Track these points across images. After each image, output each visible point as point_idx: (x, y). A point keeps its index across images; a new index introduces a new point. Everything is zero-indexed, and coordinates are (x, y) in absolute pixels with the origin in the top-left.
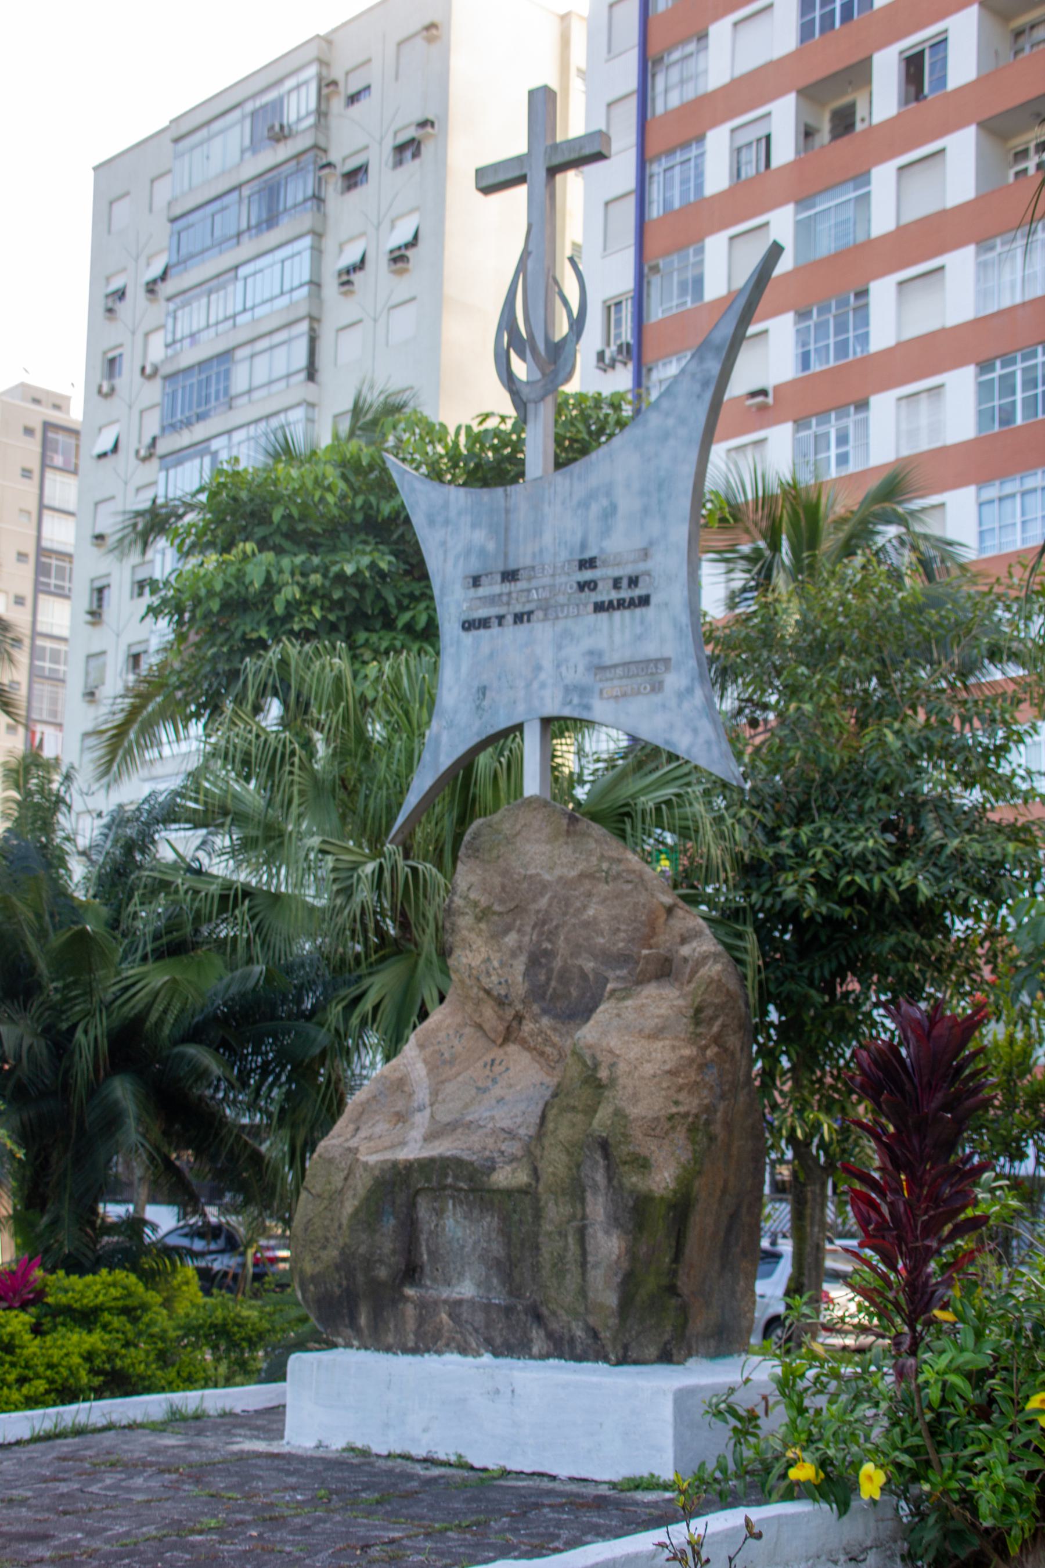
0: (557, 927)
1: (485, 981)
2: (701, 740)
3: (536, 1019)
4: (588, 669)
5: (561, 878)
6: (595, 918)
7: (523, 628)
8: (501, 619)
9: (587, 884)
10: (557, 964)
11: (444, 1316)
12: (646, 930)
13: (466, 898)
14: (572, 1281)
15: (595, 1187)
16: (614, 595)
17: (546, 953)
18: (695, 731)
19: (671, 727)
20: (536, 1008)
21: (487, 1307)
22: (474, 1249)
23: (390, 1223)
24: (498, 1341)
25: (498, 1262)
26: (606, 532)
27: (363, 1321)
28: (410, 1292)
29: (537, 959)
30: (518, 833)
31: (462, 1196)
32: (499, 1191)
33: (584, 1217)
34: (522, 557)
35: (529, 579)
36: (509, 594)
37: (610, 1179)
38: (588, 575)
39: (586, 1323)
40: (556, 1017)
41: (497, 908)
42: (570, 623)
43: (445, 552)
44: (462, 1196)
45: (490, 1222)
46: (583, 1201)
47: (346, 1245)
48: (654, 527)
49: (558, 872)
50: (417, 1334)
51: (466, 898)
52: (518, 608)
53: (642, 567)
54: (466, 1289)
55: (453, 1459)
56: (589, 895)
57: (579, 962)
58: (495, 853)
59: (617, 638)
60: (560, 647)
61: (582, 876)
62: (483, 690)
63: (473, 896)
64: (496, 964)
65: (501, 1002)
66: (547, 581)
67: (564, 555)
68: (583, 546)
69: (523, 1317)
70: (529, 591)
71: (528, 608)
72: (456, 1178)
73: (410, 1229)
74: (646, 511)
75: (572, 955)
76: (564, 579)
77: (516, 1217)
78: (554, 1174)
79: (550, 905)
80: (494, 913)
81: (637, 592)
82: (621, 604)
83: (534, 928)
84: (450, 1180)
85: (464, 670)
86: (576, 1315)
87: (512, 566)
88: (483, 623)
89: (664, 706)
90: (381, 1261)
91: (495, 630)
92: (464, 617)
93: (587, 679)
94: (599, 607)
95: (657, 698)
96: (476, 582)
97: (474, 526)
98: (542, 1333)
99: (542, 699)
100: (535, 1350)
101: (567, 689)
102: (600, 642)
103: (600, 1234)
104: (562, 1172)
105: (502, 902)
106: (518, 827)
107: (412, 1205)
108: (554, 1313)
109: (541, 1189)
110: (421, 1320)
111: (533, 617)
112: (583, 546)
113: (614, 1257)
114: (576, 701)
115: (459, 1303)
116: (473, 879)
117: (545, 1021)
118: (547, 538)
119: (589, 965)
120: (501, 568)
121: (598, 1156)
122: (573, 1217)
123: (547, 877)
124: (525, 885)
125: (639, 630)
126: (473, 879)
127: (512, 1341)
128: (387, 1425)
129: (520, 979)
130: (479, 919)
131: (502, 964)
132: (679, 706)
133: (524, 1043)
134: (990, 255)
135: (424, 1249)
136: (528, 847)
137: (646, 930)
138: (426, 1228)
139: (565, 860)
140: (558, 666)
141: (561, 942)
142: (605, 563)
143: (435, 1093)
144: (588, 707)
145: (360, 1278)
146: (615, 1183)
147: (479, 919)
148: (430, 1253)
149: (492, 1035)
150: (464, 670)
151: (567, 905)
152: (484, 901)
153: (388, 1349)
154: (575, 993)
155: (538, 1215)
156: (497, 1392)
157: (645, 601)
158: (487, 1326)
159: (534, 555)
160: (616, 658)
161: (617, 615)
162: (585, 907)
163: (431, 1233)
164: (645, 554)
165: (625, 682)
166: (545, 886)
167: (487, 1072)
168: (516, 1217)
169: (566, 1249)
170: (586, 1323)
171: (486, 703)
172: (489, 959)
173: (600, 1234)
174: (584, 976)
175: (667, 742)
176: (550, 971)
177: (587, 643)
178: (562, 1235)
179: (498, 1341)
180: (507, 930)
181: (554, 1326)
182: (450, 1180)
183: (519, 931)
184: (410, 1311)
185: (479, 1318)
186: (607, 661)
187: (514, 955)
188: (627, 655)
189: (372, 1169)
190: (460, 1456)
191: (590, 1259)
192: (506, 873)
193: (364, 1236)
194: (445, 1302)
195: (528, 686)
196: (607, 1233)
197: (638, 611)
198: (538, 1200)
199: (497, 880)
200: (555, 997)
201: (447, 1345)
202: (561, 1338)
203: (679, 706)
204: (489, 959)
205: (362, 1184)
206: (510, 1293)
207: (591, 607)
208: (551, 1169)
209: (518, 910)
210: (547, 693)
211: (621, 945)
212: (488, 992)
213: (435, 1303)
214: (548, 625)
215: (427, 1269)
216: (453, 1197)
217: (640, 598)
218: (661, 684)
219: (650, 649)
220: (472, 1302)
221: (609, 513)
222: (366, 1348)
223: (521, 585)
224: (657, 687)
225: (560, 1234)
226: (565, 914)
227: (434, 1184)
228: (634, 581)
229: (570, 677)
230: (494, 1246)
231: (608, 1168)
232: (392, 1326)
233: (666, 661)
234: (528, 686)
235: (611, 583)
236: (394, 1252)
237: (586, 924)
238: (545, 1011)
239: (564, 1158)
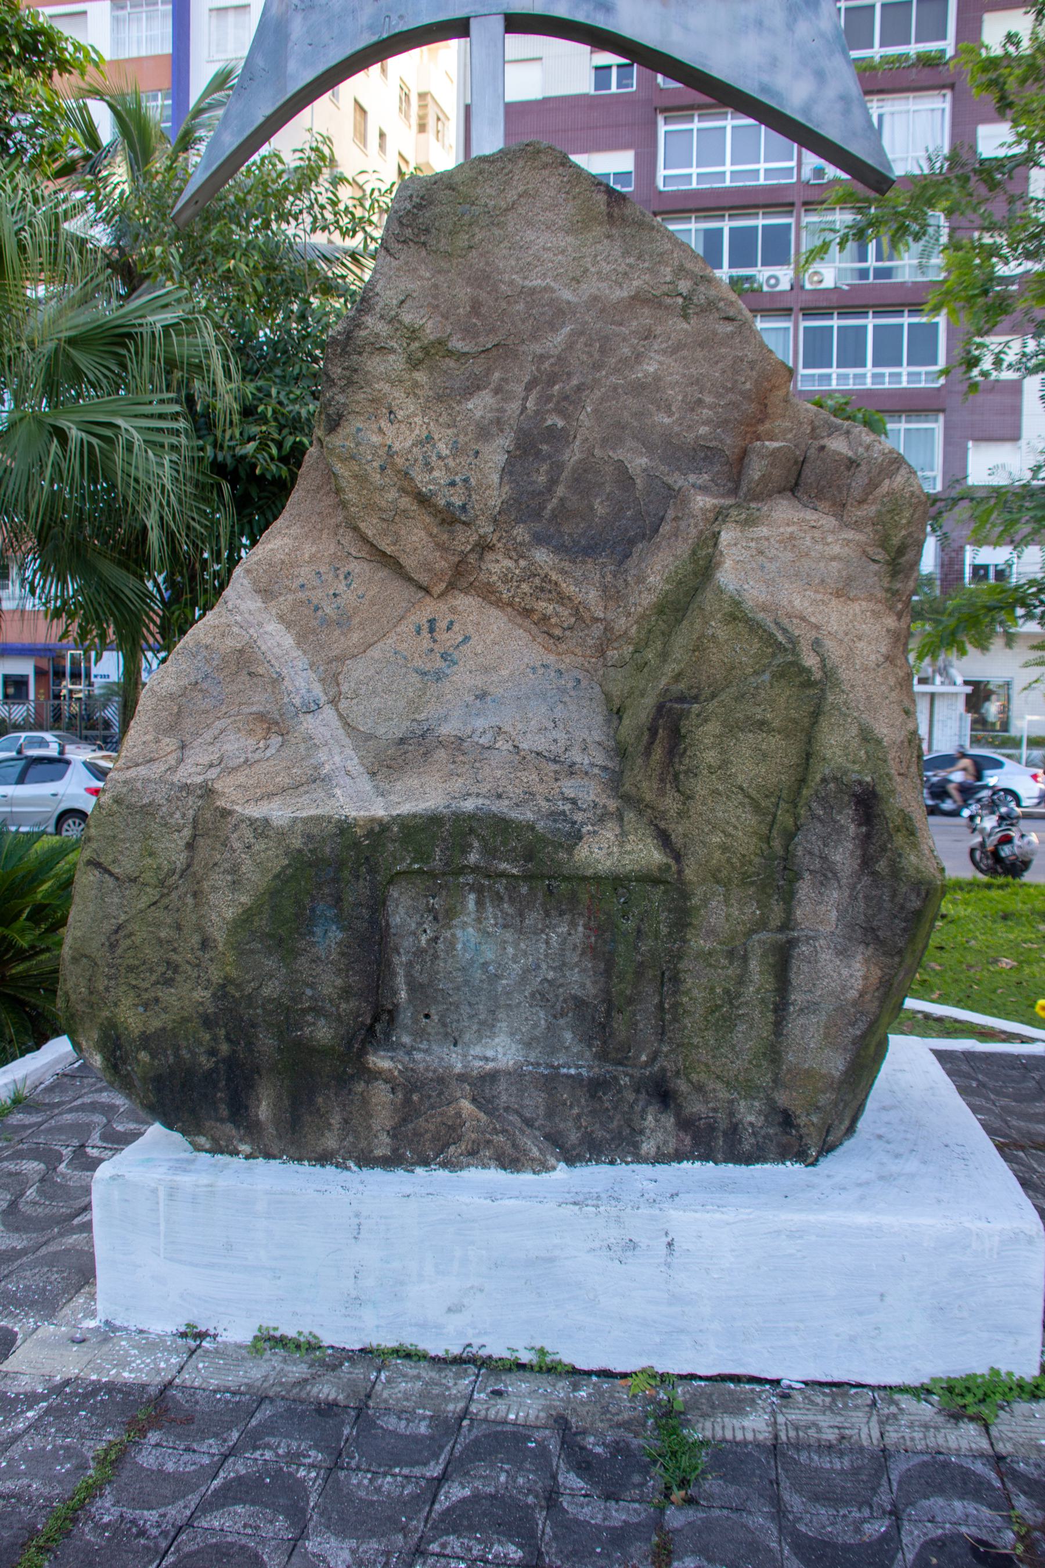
0: (579, 388)
1: (422, 480)
2: (831, 92)
3: (518, 551)
5: (596, 298)
6: (657, 378)
9: (645, 316)
10: (573, 455)
11: (466, 1105)
12: (751, 408)
13: (393, 320)
14: (749, 1036)
15: (827, 874)
17: (553, 435)
18: (820, 76)
19: (774, 63)
20: (521, 533)
21: (550, 1082)
22: (523, 980)
23: (330, 939)
24: (574, 1137)
25: (580, 1003)
27: (264, 1111)
28: (381, 1061)
29: (531, 446)
30: (512, 207)
31: (500, 886)
32: (597, 879)
33: (786, 926)
37: (867, 862)
39: (771, 1102)
40: (560, 549)
41: (457, 344)
44: (500, 886)
45: (566, 934)
46: (788, 897)
47: (228, 980)
49: (590, 287)
50: (394, 1133)
51: (393, 320)
54: (501, 1051)
55: (525, 1357)
56: (648, 335)
57: (619, 454)
61: (638, 299)
63: (407, 318)
64: (443, 449)
65: (449, 519)
69: (631, 1096)
72: (490, 852)
73: (373, 945)
75: (604, 441)
77: (630, 925)
78: (724, 848)
79: (570, 346)
80: (450, 353)
83: (529, 388)
84: (473, 858)
86: (749, 1089)
89: (759, 24)
90: (317, 1011)
98: (669, 1121)
100: (648, 1147)
103: (826, 956)
104: (746, 843)
105: (469, 332)
106: (512, 195)
107: (378, 904)
108: (700, 1088)
109: (689, 874)
110: (407, 1112)
113: (853, 994)
115: (492, 1077)
116: (408, 284)
117: (542, 556)
119: (638, 462)
121: (847, 819)
122: (762, 924)
123: (567, 295)
124: (520, 307)
126: (408, 284)
127: (599, 1134)
128: (358, 1301)
129: (495, 478)
130: (414, 364)
131: (457, 450)
132: (790, 27)
133: (488, 594)
134: (121, 13)
135: (401, 981)
136: (530, 235)
137: (751, 408)
138: (407, 943)
139: (606, 268)
141: (585, 417)
143: (332, 680)
145: (266, 1042)
146: (882, 866)
147: (414, 364)
148: (414, 987)
149: (423, 578)
151: (602, 351)
152: (432, 330)
153: (323, 1159)
154: (601, 509)
155: (682, 919)
156: (632, 1245)
158: (550, 1114)
162: (639, 357)
163: (420, 952)
166: (560, 312)
167: (426, 644)
168: (630, 925)
169: (741, 981)
170: (771, 1102)
172: (429, 438)
173: (826, 956)
174: (624, 478)
175: (765, 89)
176: (559, 466)
178: (737, 955)
179: (574, 1137)
180: (471, 390)
181: (696, 1107)
182: (473, 858)
183: (497, 391)
184: (381, 1095)
185: (535, 1102)
187: (484, 433)
189: (282, 834)
190: (542, 1352)
191: (797, 997)
192: (482, 279)
193: (270, 963)
194: (462, 1078)
196: (842, 953)
198: (685, 896)
199: (464, 293)
200: (562, 513)
201: (472, 1153)
202: (712, 1128)
203: (790, 27)
204: (429, 438)
205: (260, 866)
206: (603, 1056)
208: (716, 839)
209: (502, 351)
211: (703, 430)
212: (423, 500)
213: (441, 1080)
215: (405, 1017)
216: (479, 890)
220: (516, 1075)
222: (268, 1156)
225: (731, 954)
226: (597, 367)
227: (437, 863)
230: (574, 976)
231: (866, 840)
232: (336, 1120)
236: (346, 993)
237: (639, 388)
238: (539, 540)
239: (749, 818)
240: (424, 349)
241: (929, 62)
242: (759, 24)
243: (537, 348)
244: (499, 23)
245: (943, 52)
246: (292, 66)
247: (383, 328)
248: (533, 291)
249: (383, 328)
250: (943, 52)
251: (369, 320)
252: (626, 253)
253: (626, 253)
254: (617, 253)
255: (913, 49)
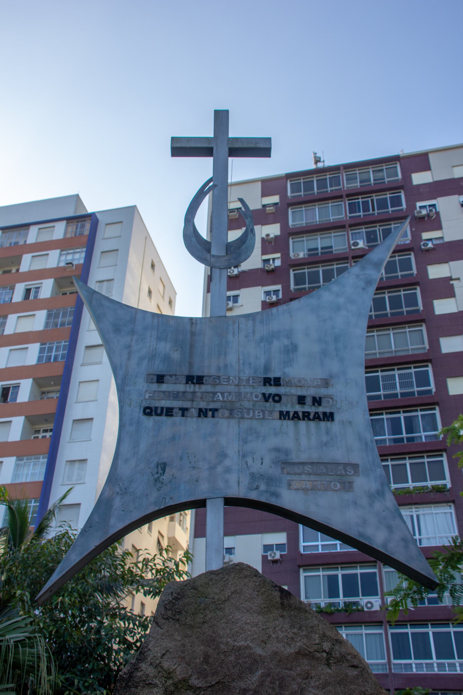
4: (276, 462)
5: (276, 653)
7: (206, 423)
8: (184, 411)
13: (158, 666)
16: (298, 408)
19: (365, 522)
26: (288, 362)
30: (228, 599)
34: (208, 367)
35: (214, 385)
36: (194, 393)
38: (273, 390)
41: (194, 681)
42: (255, 424)
43: (130, 353)
48: (334, 366)
49: (273, 646)
51: (158, 666)
52: (203, 405)
53: (322, 392)
56: (307, 677)
58: (200, 618)
59: (304, 442)
60: (245, 442)
61: (300, 654)
62: (163, 467)
63: (166, 665)
66: (231, 388)
67: (247, 373)
68: (267, 368)
70: (214, 393)
71: (212, 406)
74: (324, 353)
76: (248, 390)
79: (262, 684)
80: (190, 687)
81: (321, 410)
82: (306, 416)
85: (143, 446)
87: (196, 372)
88: (169, 412)
91: (178, 419)
92: (145, 404)
93: (275, 471)
94: (284, 415)
95: (348, 496)
96: (160, 379)
97: (159, 339)
99: (227, 481)
101: (253, 476)
102: (288, 442)
105: (202, 674)
106: (227, 593)
111: (220, 413)
112: (267, 368)
114: (263, 487)
118: (232, 358)
120: (186, 373)
123: (259, 651)
124: (232, 658)
125: (325, 438)
134: (20, 462)
139: (281, 635)
140: (244, 456)
142: (289, 384)
144: (276, 495)
150: (143, 446)
151: (281, 686)
152: (180, 672)
157: (329, 417)
159: (219, 369)
160: (303, 457)
161: (302, 424)
164: (326, 383)
165: (313, 477)
166: (256, 662)
171: (166, 477)
175: (361, 535)
177: (273, 442)
186: (294, 458)
188: (314, 456)
195: (212, 468)
197: (323, 424)
199: (200, 649)
207: (277, 415)
210: (233, 478)
214: (233, 422)
217: (325, 414)
218: (351, 483)
219: (337, 454)
221: (291, 350)
223: (204, 388)
224: (348, 486)
228: (317, 401)
229: (256, 467)
233: (355, 466)
234: (212, 468)
235: (295, 399)
240: (175, 684)
241: (439, 490)
242: (355, 503)
243: (242, 684)
244: (220, 503)
245: (445, 485)
246: (113, 521)
247: (151, 671)
248: (239, 649)
249: (151, 671)
250: (445, 485)
251: (143, 666)
252: (292, 626)
253: (292, 626)
254: (287, 626)
255: (430, 483)
